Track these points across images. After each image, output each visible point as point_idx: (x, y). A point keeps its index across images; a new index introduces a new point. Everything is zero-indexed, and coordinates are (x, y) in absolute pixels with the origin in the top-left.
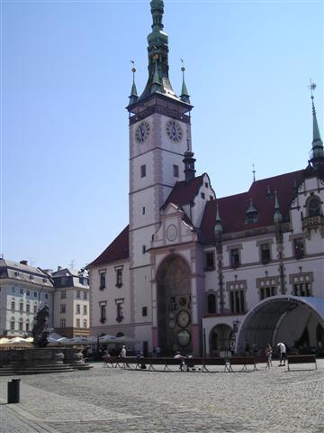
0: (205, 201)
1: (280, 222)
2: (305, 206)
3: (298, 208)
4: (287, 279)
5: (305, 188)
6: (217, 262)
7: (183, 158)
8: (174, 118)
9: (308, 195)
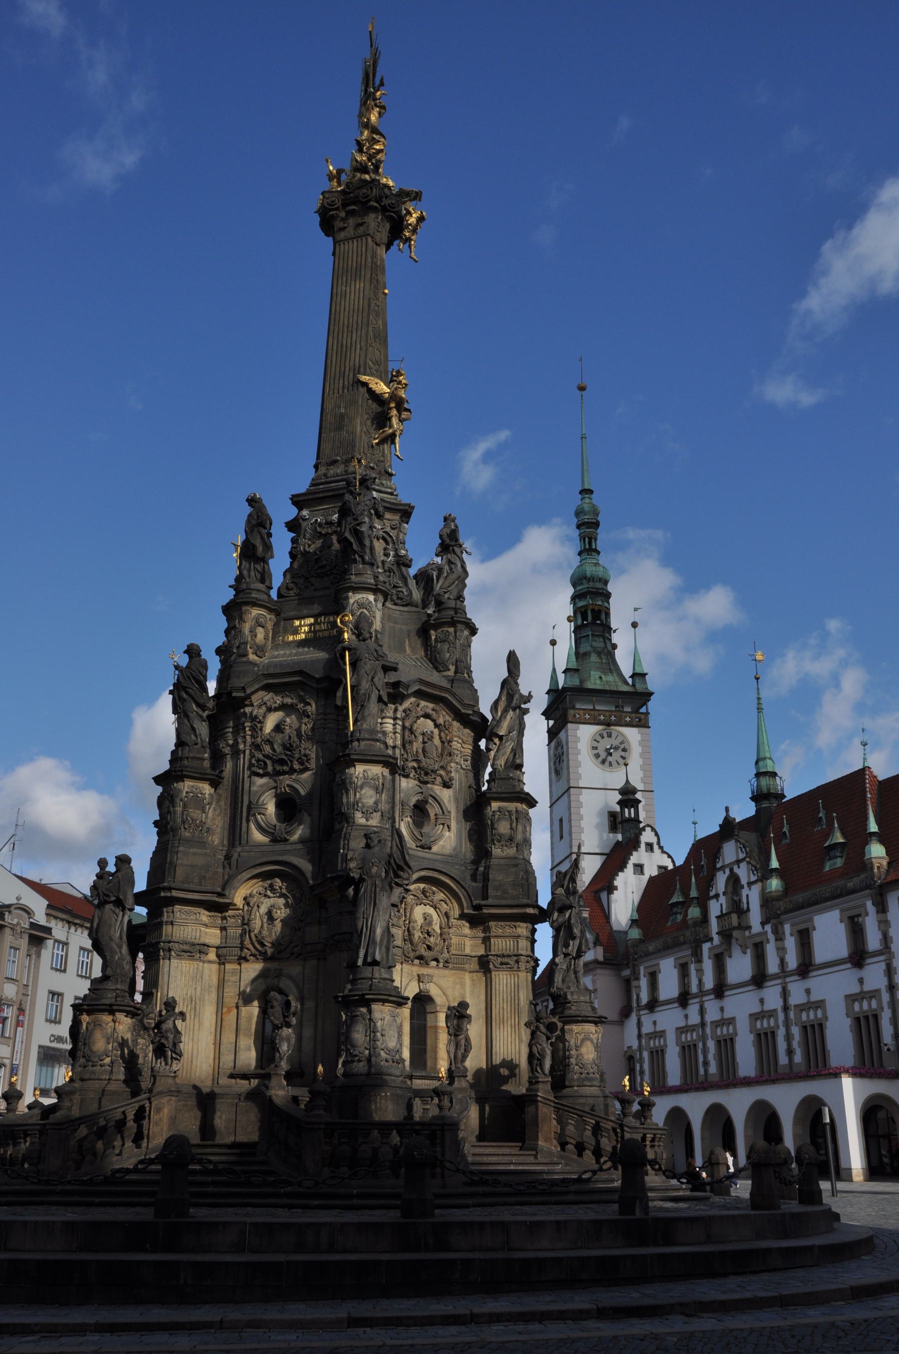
0: (645, 878)
2: (724, 894)
3: (717, 896)
4: (708, 1030)
5: (723, 861)
6: (635, 997)
8: (609, 725)
9: (727, 871)
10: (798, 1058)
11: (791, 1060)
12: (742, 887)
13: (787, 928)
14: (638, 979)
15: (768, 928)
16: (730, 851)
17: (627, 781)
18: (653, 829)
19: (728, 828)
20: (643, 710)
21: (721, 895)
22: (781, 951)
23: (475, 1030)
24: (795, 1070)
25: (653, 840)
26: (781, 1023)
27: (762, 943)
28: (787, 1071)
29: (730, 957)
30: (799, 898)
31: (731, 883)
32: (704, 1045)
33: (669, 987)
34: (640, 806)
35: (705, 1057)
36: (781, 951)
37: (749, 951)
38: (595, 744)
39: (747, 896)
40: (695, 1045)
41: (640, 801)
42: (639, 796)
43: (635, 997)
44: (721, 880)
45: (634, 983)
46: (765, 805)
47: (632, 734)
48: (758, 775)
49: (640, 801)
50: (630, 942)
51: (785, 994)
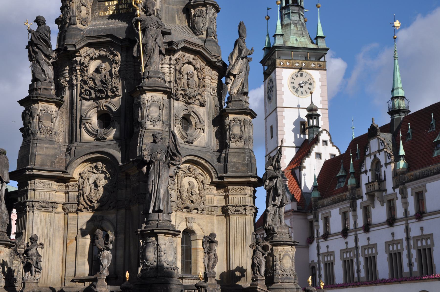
0: (322, 162)
1: (352, 188)
2: (370, 170)
3: (366, 172)
4: (360, 251)
5: (370, 151)
6: (316, 232)
7: (307, 113)
8: (301, 69)
9: (373, 157)
10: (415, 268)
11: (411, 269)
12: (382, 166)
13: (409, 191)
14: (317, 221)
15: (397, 190)
16: (374, 145)
17: (312, 103)
18: (327, 132)
19: (373, 132)
20: (322, 59)
21: (368, 171)
22: (405, 204)
23: (220, 250)
24: (414, 275)
25: (327, 138)
26: (405, 247)
27: (393, 200)
28: (409, 276)
29: (374, 208)
30: (417, 172)
31: (375, 164)
32: (358, 260)
33: (336, 225)
34: (320, 118)
35: (358, 267)
36: (405, 204)
37: (385, 204)
38: (293, 81)
39: (385, 172)
40: (352, 260)
41: (319, 115)
42: (319, 112)
43: (316, 232)
44: (369, 162)
45: (315, 224)
46: (397, 116)
47: (316, 75)
48: (393, 98)
49: (319, 115)
50: (312, 199)
51: (407, 230)
